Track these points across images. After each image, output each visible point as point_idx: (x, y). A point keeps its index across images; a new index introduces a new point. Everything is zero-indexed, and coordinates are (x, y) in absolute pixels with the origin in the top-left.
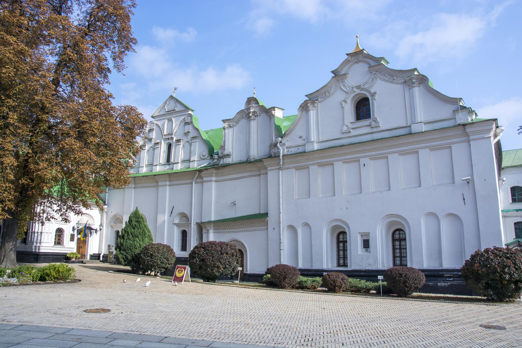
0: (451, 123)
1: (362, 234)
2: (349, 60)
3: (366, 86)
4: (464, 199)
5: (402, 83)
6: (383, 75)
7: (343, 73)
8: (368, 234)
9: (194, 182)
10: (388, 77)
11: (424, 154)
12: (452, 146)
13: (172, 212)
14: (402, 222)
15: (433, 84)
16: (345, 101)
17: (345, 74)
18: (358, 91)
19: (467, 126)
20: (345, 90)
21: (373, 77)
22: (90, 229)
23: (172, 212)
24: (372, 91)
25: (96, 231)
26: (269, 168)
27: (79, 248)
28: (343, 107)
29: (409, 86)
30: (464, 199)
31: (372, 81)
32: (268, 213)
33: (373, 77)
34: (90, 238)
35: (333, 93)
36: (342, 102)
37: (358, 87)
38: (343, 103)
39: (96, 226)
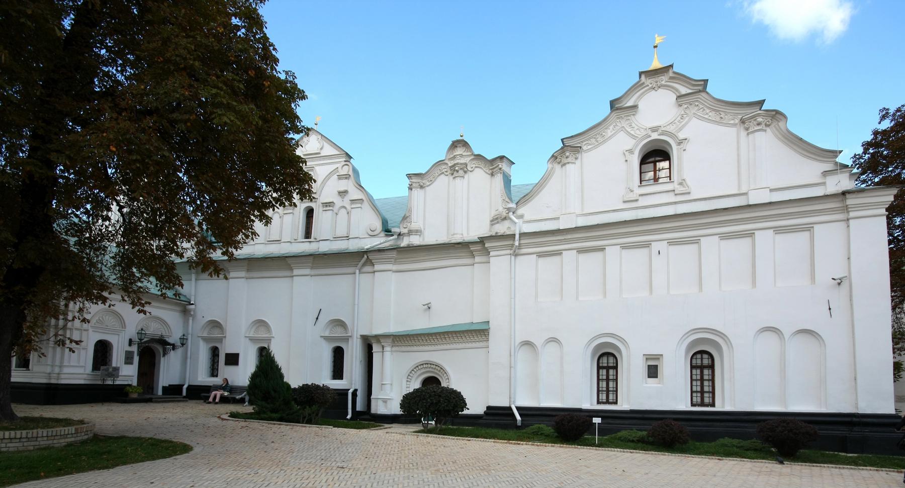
0: (818, 192)
1: (648, 357)
2: (644, 83)
3: (671, 129)
4: (830, 309)
5: (734, 125)
6: (701, 110)
7: (630, 104)
8: (658, 357)
9: (357, 271)
10: (710, 114)
11: (764, 238)
12: (816, 227)
13: (317, 318)
14: (716, 339)
15: (795, 126)
16: (631, 151)
17: (635, 107)
18: (655, 136)
19: (848, 196)
20: (632, 132)
21: (683, 112)
22: (163, 342)
23: (317, 318)
24: (681, 136)
25: (174, 347)
26: (492, 254)
27: (141, 374)
28: (626, 161)
29: (747, 129)
30: (830, 309)
31: (682, 120)
32: (489, 322)
33: (683, 112)
34: (162, 359)
35: (610, 137)
36: (625, 152)
37: (654, 129)
38: (627, 153)
39: (174, 338)
